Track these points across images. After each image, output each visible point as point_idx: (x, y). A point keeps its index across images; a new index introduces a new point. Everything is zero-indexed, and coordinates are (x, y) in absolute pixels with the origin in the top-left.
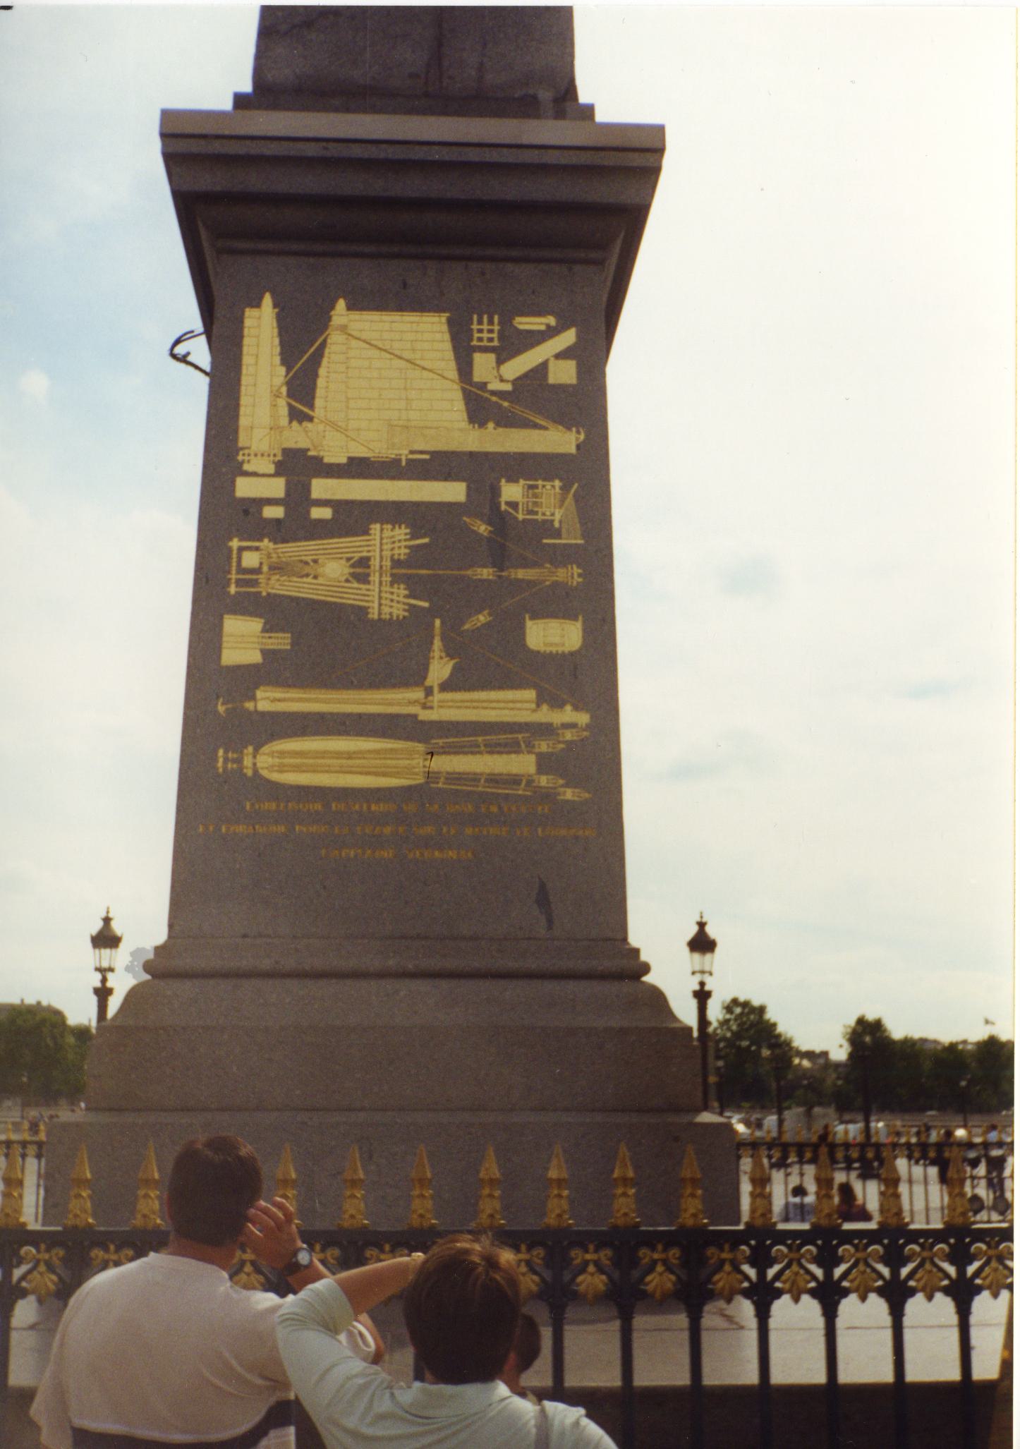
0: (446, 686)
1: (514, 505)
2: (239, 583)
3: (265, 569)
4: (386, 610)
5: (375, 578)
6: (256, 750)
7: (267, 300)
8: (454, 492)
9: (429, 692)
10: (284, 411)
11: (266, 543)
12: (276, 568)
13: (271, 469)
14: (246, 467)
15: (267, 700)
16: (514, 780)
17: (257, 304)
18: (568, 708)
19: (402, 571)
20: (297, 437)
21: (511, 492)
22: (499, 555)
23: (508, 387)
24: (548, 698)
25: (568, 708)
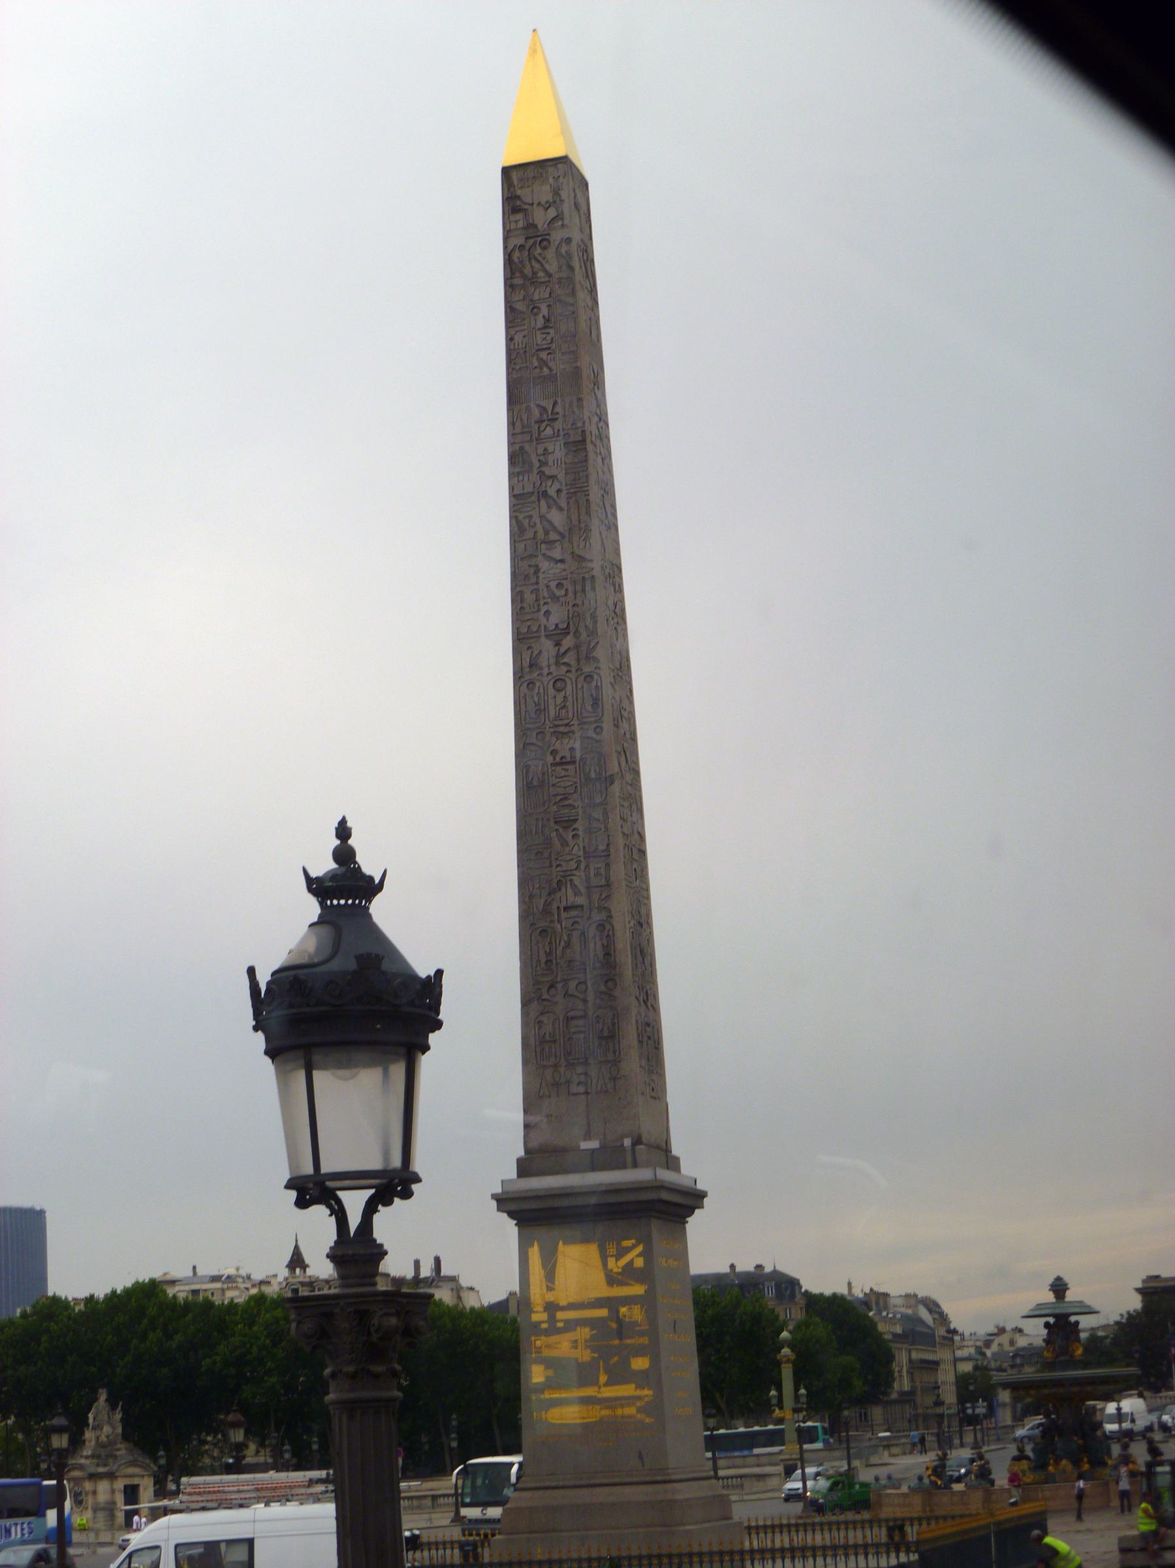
0: (606, 1385)
1: (625, 1316)
2: (535, 1353)
3: (543, 1346)
4: (584, 1359)
6: (546, 1411)
7: (536, 1244)
8: (603, 1313)
9: (600, 1388)
10: (544, 1287)
11: (543, 1338)
12: (548, 1346)
13: (542, 1310)
14: (534, 1309)
15: (547, 1395)
16: (630, 1417)
17: (532, 1246)
18: (646, 1389)
19: (590, 1344)
20: (550, 1297)
21: (623, 1310)
22: (620, 1334)
23: (620, 1270)
24: (639, 1387)
25: (646, 1389)
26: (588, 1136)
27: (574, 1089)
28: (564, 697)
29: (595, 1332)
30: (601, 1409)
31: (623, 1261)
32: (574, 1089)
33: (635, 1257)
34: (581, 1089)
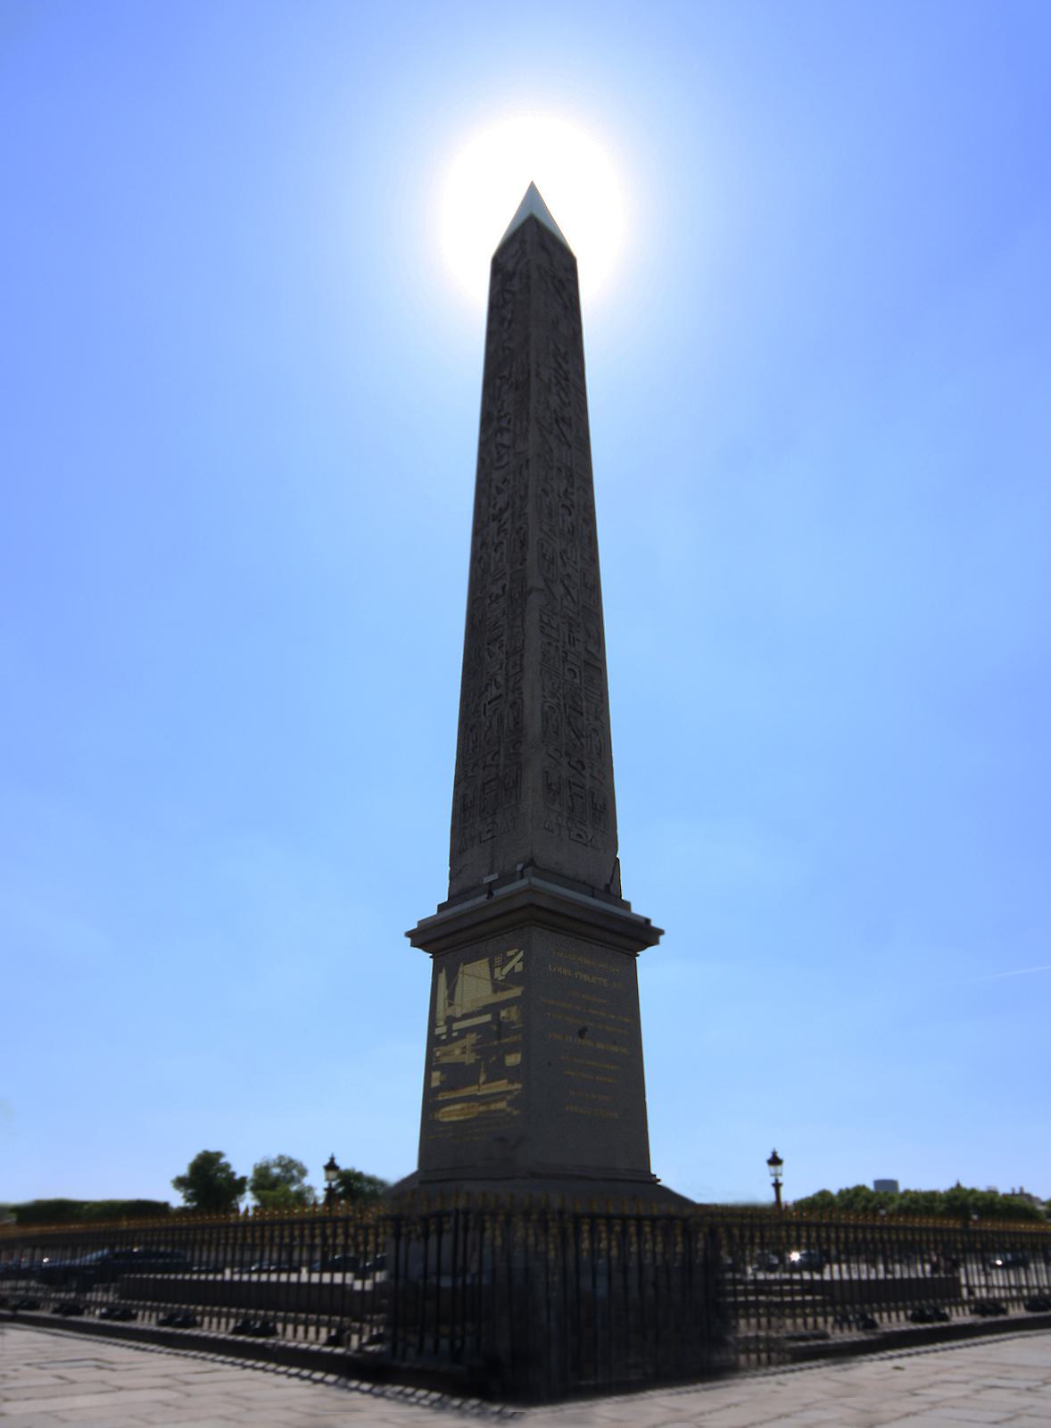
0: (484, 1083)
1: (503, 1018)
5: (468, 1052)
8: (487, 1018)
9: (479, 1086)
10: (447, 1002)
19: (476, 1049)
21: (503, 1014)
22: (499, 1036)
23: (504, 977)
24: (511, 1082)
26: (491, 872)
27: (484, 837)
28: (502, 553)
29: (479, 1037)
30: (479, 1106)
31: (506, 970)
32: (484, 837)
33: (516, 964)
34: (489, 835)
